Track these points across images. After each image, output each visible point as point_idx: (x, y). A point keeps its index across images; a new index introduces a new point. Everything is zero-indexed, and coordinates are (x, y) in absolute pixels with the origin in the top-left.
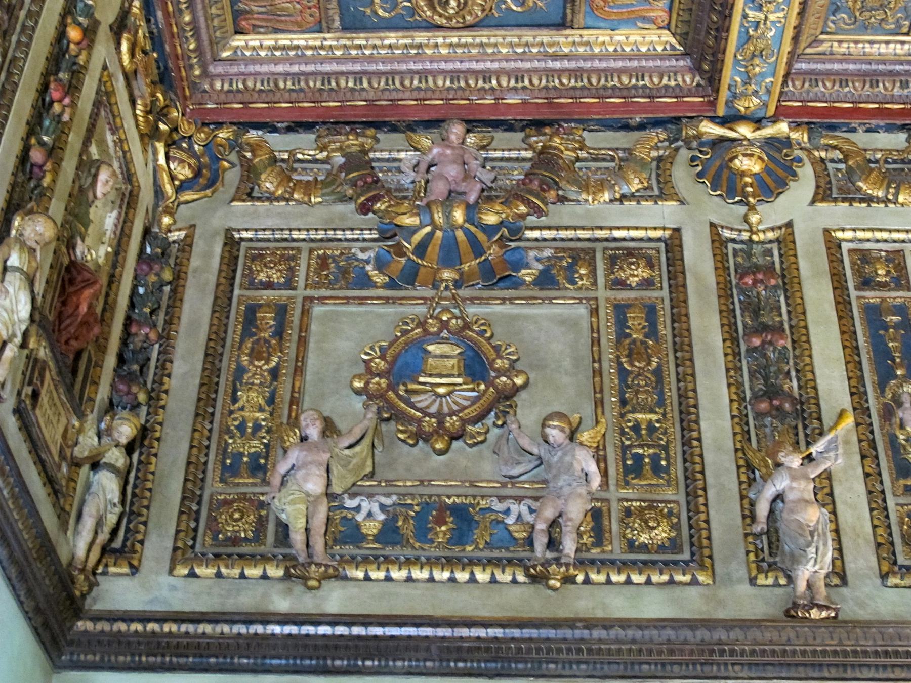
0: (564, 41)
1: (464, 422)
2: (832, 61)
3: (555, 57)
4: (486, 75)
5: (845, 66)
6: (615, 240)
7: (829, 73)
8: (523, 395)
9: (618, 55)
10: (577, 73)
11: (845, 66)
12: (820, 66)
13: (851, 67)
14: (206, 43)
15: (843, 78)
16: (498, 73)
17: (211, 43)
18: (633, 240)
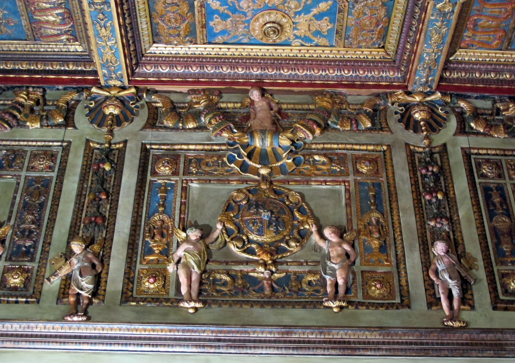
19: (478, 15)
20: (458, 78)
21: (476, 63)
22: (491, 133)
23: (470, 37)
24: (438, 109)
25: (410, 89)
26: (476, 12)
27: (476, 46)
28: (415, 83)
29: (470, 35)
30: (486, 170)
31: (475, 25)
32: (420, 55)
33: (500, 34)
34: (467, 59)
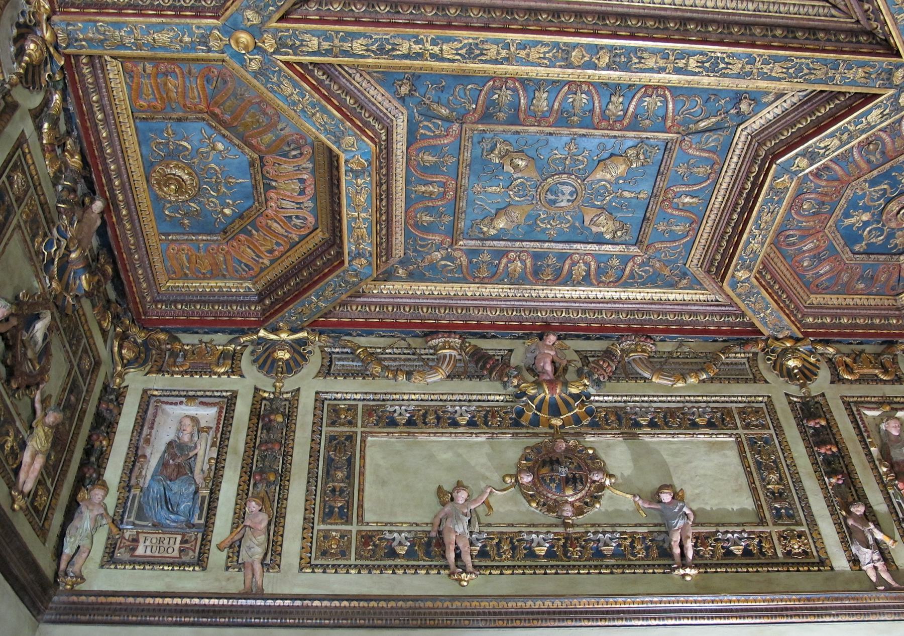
19: (183, 73)
20: (84, 75)
21: (110, 90)
22: (47, 155)
23: (144, 71)
24: (45, 71)
25: (55, 18)
26: (186, 70)
27: (132, 82)
28: (68, 24)
29: (148, 71)
30: (18, 177)
31: (166, 74)
32: (124, 23)
33: (159, 105)
34: (111, 76)
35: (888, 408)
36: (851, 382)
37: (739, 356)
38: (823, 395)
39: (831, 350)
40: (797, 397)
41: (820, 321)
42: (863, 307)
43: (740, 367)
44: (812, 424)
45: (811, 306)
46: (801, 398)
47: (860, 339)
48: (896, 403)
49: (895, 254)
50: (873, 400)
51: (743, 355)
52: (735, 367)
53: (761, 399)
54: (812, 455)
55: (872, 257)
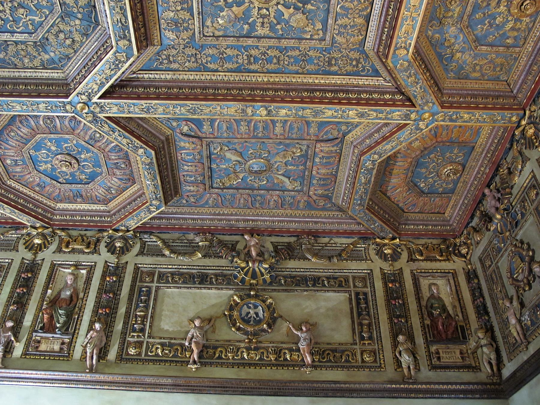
0: (478, 149)
1: (527, 278)
2: (518, 82)
3: (482, 153)
4: (478, 173)
5: (521, 79)
6: (526, 187)
7: (521, 85)
8: (536, 256)
9: (488, 138)
10: (488, 152)
11: (521, 79)
12: (518, 86)
13: (522, 77)
14: (441, 223)
15: (524, 82)
16: (479, 169)
17: (443, 221)
18: (528, 183)
35: (73, 268)
36: (65, 252)
37: (13, 235)
38: (43, 259)
39: (63, 234)
40: (27, 260)
41: (62, 218)
42: (88, 211)
43: (11, 242)
44: (23, 276)
45: (59, 210)
46: (29, 261)
47: (84, 228)
48: (83, 265)
49: (86, 184)
50: (70, 263)
51: (16, 236)
52: (8, 242)
53: (7, 261)
54: (12, 292)
55: (73, 185)
